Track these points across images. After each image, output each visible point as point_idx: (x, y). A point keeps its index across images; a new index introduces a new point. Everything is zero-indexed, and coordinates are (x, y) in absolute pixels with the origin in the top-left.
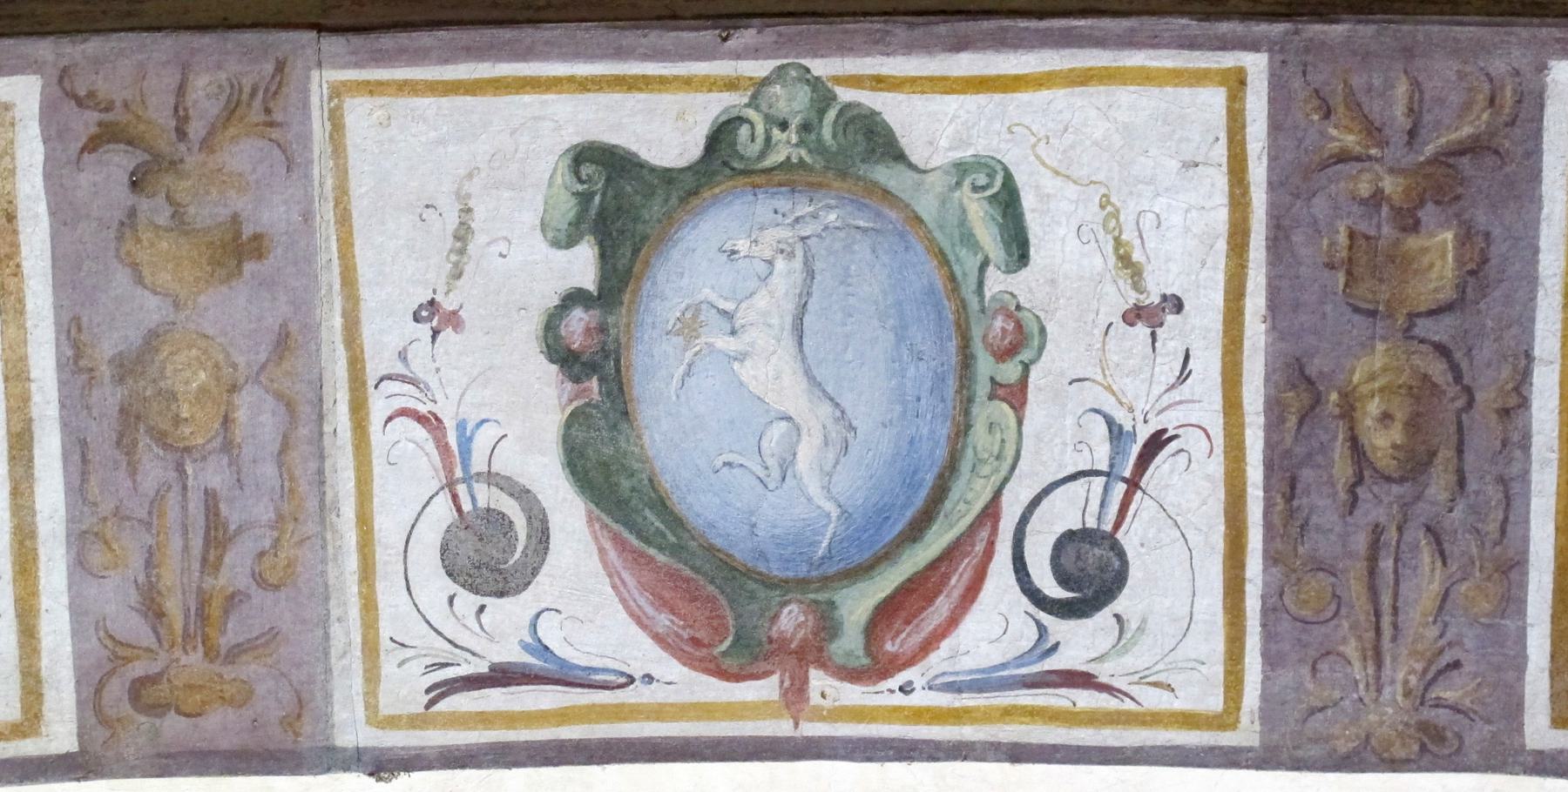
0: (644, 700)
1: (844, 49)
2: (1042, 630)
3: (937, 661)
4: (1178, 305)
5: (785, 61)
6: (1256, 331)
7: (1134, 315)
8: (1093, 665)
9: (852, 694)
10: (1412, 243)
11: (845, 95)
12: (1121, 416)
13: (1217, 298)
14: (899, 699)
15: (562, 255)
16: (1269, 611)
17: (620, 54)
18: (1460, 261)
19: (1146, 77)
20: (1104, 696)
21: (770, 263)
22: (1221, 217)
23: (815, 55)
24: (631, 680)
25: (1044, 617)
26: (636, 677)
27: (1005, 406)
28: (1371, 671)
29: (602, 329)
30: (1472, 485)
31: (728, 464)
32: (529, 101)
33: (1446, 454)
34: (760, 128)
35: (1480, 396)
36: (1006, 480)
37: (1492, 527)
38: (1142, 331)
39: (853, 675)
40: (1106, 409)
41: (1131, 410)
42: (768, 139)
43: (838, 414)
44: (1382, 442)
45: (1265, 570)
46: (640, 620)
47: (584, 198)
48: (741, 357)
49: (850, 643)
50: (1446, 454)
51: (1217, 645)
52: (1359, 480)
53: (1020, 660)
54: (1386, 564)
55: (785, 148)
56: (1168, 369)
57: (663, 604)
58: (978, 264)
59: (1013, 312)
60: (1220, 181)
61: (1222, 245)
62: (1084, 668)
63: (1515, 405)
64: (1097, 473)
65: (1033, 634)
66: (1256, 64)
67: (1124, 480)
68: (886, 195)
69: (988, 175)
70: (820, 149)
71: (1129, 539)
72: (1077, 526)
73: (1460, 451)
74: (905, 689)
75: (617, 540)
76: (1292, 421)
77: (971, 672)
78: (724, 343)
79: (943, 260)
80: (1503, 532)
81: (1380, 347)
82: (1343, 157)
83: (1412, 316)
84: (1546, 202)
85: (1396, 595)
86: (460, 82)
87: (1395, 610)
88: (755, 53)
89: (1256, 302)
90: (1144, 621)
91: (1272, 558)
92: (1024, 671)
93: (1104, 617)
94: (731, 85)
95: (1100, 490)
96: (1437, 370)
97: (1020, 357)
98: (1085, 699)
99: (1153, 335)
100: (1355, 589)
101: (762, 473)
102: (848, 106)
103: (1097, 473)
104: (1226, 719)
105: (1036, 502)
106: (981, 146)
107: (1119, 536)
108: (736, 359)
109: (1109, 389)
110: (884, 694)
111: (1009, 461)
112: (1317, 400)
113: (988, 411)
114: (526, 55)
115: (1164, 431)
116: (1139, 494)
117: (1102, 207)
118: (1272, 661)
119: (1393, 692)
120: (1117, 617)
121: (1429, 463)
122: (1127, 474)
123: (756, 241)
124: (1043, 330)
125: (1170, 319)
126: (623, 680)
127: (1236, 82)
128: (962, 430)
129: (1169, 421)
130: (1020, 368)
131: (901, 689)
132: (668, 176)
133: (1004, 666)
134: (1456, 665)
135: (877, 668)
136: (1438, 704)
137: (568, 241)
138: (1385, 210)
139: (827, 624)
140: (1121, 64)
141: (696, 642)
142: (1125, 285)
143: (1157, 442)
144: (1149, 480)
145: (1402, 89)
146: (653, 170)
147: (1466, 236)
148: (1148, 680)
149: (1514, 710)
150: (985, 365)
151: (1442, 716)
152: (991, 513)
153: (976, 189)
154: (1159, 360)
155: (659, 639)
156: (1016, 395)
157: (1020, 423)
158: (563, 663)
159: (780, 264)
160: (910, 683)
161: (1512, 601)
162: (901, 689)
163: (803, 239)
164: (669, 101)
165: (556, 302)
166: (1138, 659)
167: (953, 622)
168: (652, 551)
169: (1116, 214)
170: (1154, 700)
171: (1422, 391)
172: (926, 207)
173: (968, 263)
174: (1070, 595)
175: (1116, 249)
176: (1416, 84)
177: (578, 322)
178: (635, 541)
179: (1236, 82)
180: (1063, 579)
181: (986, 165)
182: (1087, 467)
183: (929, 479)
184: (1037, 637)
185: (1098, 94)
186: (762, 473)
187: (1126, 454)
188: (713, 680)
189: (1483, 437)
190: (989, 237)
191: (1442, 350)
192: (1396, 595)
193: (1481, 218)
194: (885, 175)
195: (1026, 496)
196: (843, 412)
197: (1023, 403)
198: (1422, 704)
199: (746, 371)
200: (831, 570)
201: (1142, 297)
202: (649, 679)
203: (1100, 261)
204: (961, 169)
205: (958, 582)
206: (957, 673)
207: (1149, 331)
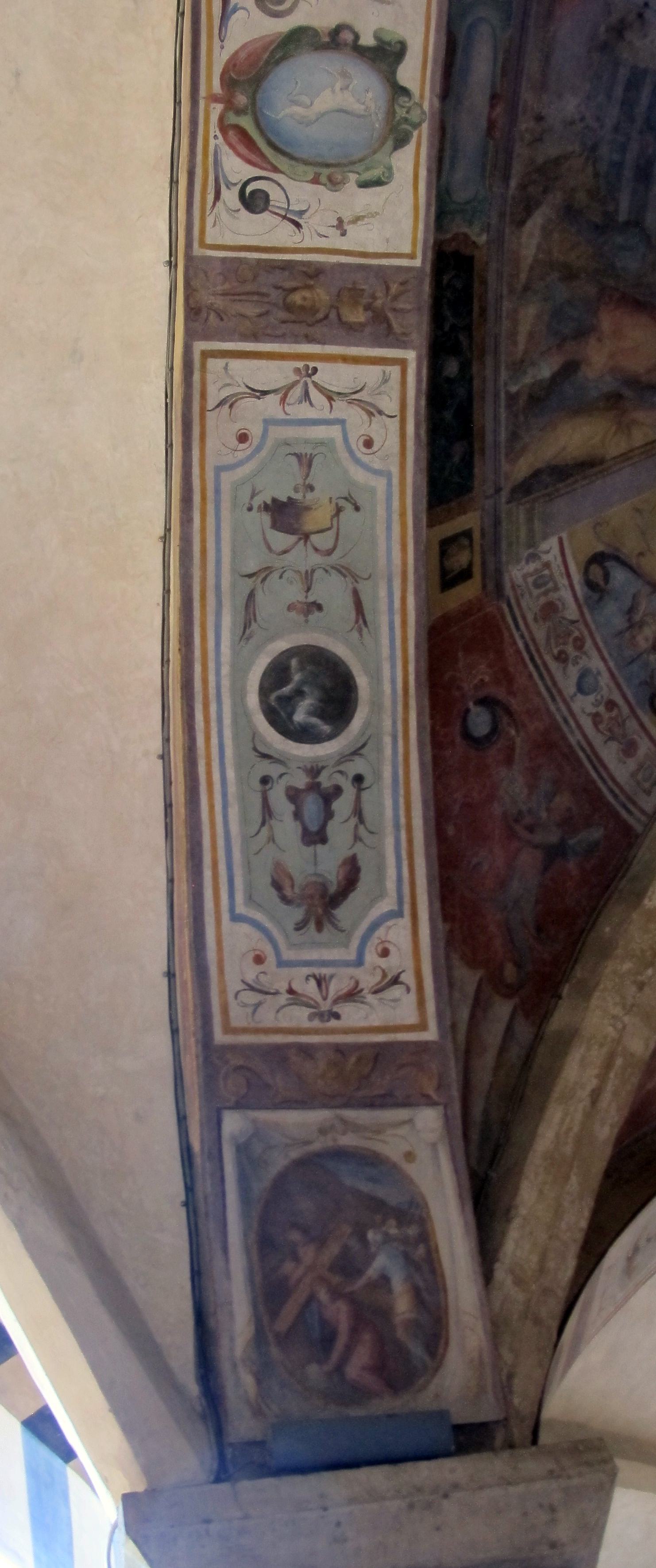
0: (214, 45)
1: (431, 136)
2: (235, 184)
3: (225, 149)
4: (344, 234)
5: (427, 115)
6: (334, 259)
7: (340, 221)
8: (222, 201)
9: (214, 118)
10: (361, 309)
11: (415, 133)
12: (307, 214)
13: (345, 248)
14: (212, 135)
15: (371, 34)
16: (240, 260)
17: (435, 61)
18: (354, 323)
19: (415, 228)
20: (212, 204)
21: (363, 104)
22: (371, 249)
23: (429, 124)
24: (222, 41)
25: (239, 186)
26: (223, 43)
27: (311, 177)
28: (220, 292)
29: (346, 45)
30: (284, 326)
31: (297, 83)
32: (423, 29)
33: (293, 317)
34: (408, 105)
35: (310, 329)
36: (287, 176)
37: (269, 331)
38: (335, 223)
39: (221, 119)
40: (310, 210)
41: (309, 218)
42: (403, 107)
43: (312, 122)
44: (297, 298)
45: (255, 259)
46: (244, 46)
47: (389, 44)
48: (333, 91)
49: (232, 119)
50: (293, 317)
51: (229, 242)
52: (284, 290)
53: (225, 177)
54: (255, 298)
55: (401, 113)
56: (323, 230)
57: (249, 55)
58: (359, 172)
59: (343, 182)
60: (381, 250)
61: (362, 249)
62: (221, 198)
63: (309, 339)
64: (289, 205)
65: (234, 181)
66: (417, 263)
67: (286, 214)
68: (383, 144)
69: (388, 177)
70: (399, 123)
71: (266, 215)
72: (271, 198)
73: (294, 322)
74: (216, 137)
75: (272, 42)
76: (305, 269)
77: (221, 158)
78: (338, 86)
79: (361, 160)
80: (268, 335)
81: (328, 298)
82: (388, 288)
83: (337, 308)
84: (373, 349)
85: (246, 301)
86: (431, 7)
87: (240, 301)
88: (431, 105)
89: (344, 259)
90: (238, 218)
91: (259, 261)
92: (221, 178)
93: (238, 205)
94: (422, 96)
95: (283, 206)
96: (320, 315)
97: (328, 183)
98: (211, 197)
99: (334, 226)
100: (248, 287)
101: (294, 93)
102: (412, 134)
103: (289, 205)
104: (203, 244)
105: (279, 185)
106: (396, 175)
107: (267, 213)
108: (332, 89)
109: (316, 211)
110: (214, 129)
111: (293, 177)
112: (311, 277)
113: (310, 172)
114: (437, 31)
115: (302, 229)
116: (281, 219)
117: (375, 212)
118: (224, 260)
119: (212, 300)
120: (239, 210)
121: (290, 312)
122: (288, 216)
123: (371, 99)
124: (336, 191)
125: (339, 232)
126: (222, 38)
127: (412, 256)
128: (306, 163)
129: (305, 230)
130: (325, 183)
131: (215, 136)
132: (394, 73)
133: (222, 170)
134: (222, 319)
135: (224, 128)
136: (208, 315)
137: (377, 37)
138: (371, 300)
139: (239, 112)
140: (420, 221)
141: (235, 65)
142: (350, 218)
143: (298, 225)
144: (286, 222)
145: (408, 307)
146: (397, 68)
147: (362, 325)
148: (217, 219)
149: (207, 337)
150: (326, 172)
151: (204, 315)
152: (276, 170)
153: (383, 173)
154: (325, 228)
155: (236, 53)
156: (315, 181)
157: (307, 182)
158: (229, 18)
159: (363, 107)
160: (218, 138)
161: (244, 338)
162: (215, 136)
163: (371, 115)
164: (418, 75)
165: (356, 30)
166: (224, 216)
167: (239, 154)
168: (268, 54)
169: (373, 216)
170: (210, 221)
171: (313, 310)
172: (378, 156)
173: (359, 167)
174: (247, 195)
175: (362, 216)
176: (409, 311)
177: (347, 36)
178: (272, 47)
179: (412, 256)
180: (253, 193)
181: (390, 177)
182: (291, 203)
183: (288, 150)
184: (233, 182)
185: (411, 214)
186: (294, 93)
187: (295, 215)
188: (221, 70)
189: (296, 328)
190: (367, 176)
191: (326, 317)
192: (246, 301)
193: (368, 330)
194: (390, 143)
195: (282, 182)
196: (313, 123)
197: (313, 183)
198: (208, 309)
199: (328, 92)
200: (259, 114)
201: (346, 224)
202: (222, 47)
203: (359, 210)
204: (390, 169)
205: (253, 157)
206: (221, 155)
207: (335, 225)
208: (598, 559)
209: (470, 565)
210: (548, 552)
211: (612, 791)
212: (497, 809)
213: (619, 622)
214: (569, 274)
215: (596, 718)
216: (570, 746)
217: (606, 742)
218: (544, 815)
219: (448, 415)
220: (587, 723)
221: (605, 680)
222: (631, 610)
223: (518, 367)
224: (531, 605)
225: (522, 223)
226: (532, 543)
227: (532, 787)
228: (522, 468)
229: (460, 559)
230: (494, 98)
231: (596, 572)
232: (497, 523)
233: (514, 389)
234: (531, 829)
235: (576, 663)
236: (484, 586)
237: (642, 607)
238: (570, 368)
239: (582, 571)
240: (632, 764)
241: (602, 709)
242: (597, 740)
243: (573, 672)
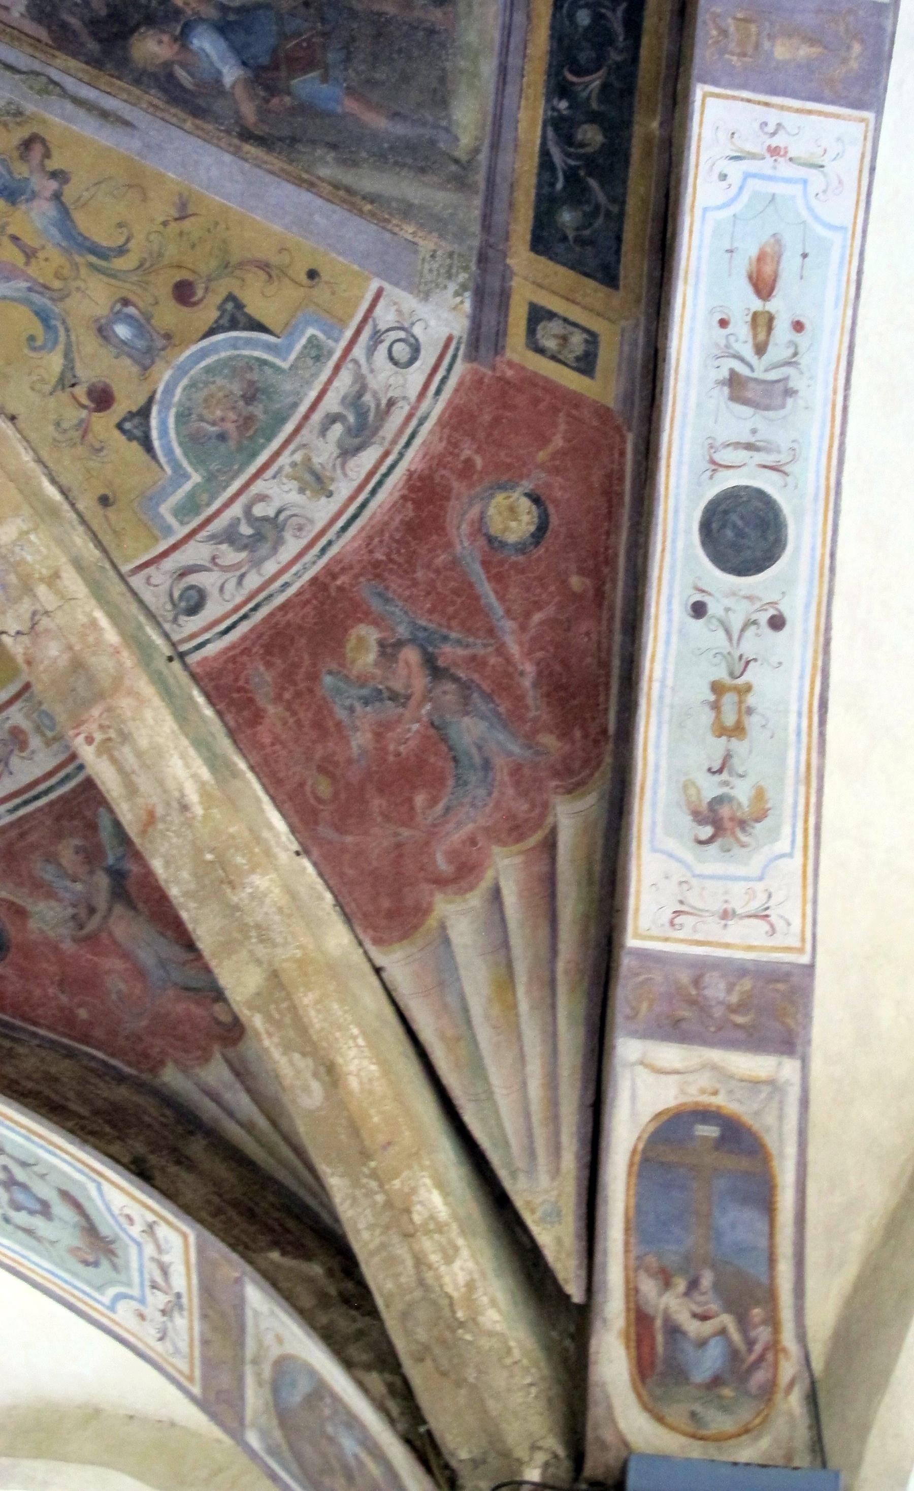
211: (62, 782)
212: (68, 946)
216: (12, 825)
217: (11, 773)
218: (79, 887)
227: (51, 894)
234: (92, 910)
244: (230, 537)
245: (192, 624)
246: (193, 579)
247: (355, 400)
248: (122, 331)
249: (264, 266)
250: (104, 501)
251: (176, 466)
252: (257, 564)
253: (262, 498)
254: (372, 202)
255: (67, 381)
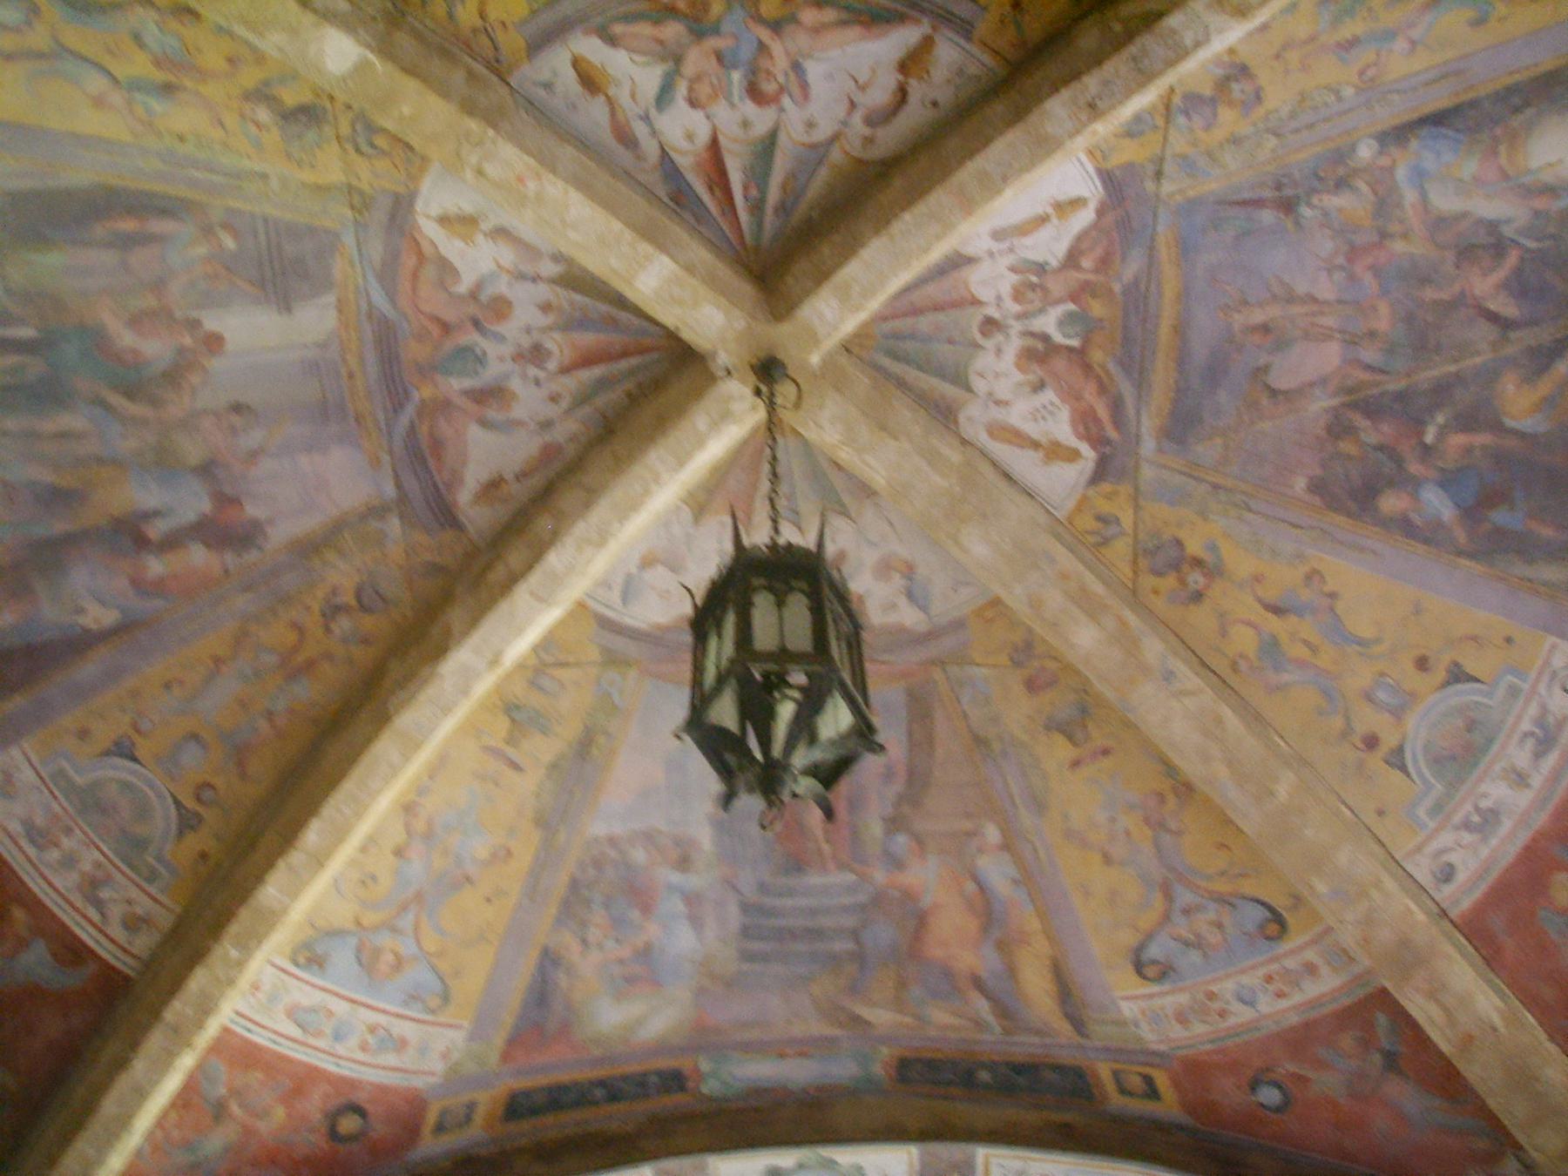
208: (1139, 968)
209: (1140, 1074)
210: (1131, 1010)
213: (1195, 956)
214: (902, 984)
215: (1280, 995)
219: (1021, 1080)
220: (1284, 1004)
221: (1245, 980)
222: (1187, 944)
223: (979, 1024)
224: (1177, 1032)
225: (868, 1023)
226: (1121, 1023)
228: (1065, 1028)
229: (1135, 1082)
230: (782, 1056)
231: (1151, 971)
232: (1107, 1049)
233: (998, 1029)
235: (1228, 1003)
236: (1158, 1066)
237: (1184, 933)
238: (978, 983)
239: (1149, 983)
240: (1324, 970)
241: (1271, 988)
242: (1297, 998)
243: (1236, 1006)
244: (1467, 826)
245: (1448, 889)
246: (1446, 858)
247: (1540, 722)
248: (1382, 695)
249: (1474, 638)
250: (1380, 813)
251: (1425, 781)
252: (1484, 840)
253: (1485, 795)
254: (1544, 585)
255: (1346, 734)
